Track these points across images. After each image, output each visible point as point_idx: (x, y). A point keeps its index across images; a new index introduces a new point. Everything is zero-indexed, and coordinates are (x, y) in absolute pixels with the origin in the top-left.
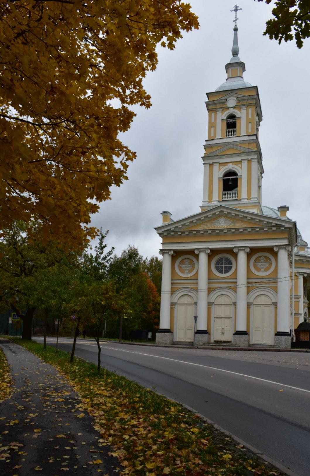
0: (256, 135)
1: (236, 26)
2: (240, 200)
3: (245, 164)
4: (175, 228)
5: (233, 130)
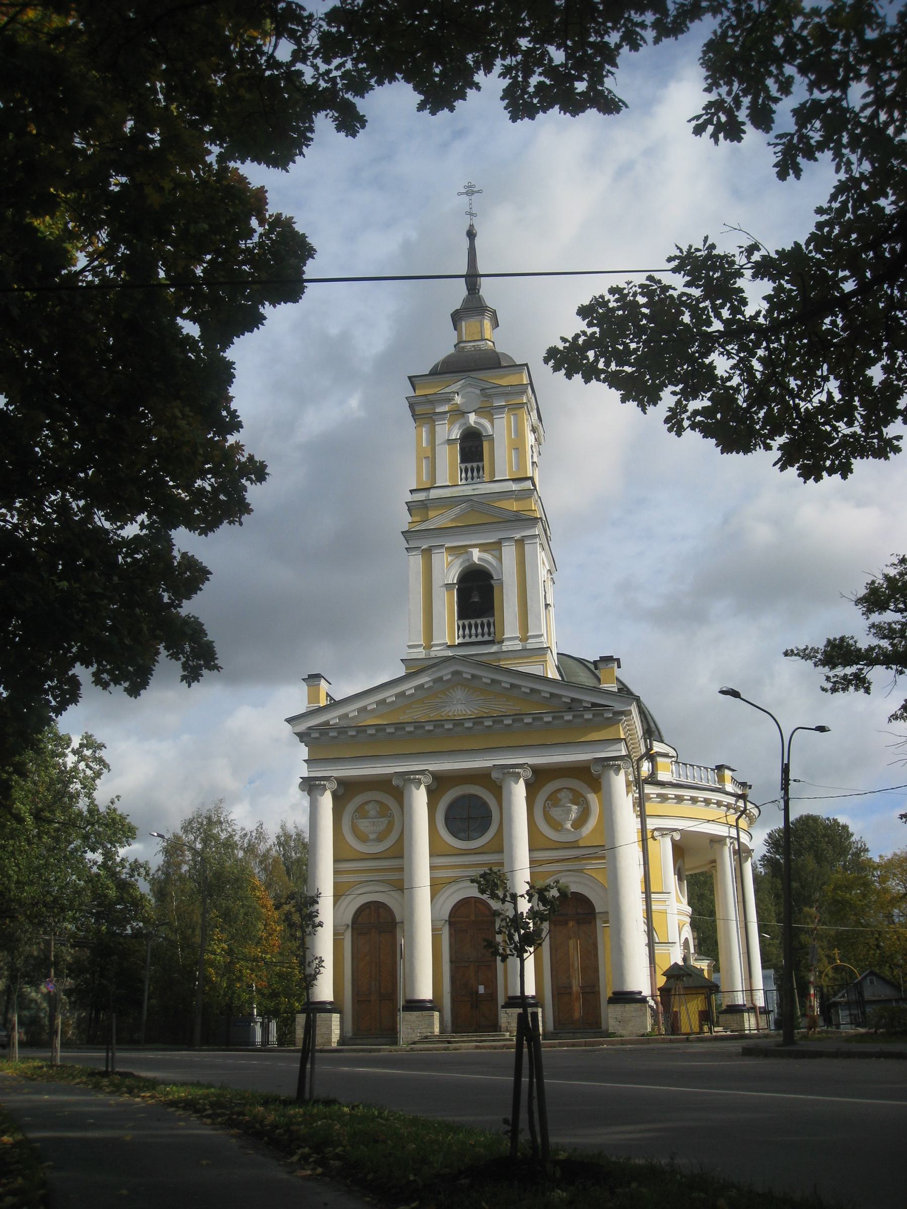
0: (531, 479)
1: (472, 226)
2: (501, 642)
3: (509, 552)
4: (340, 718)
5: (475, 465)
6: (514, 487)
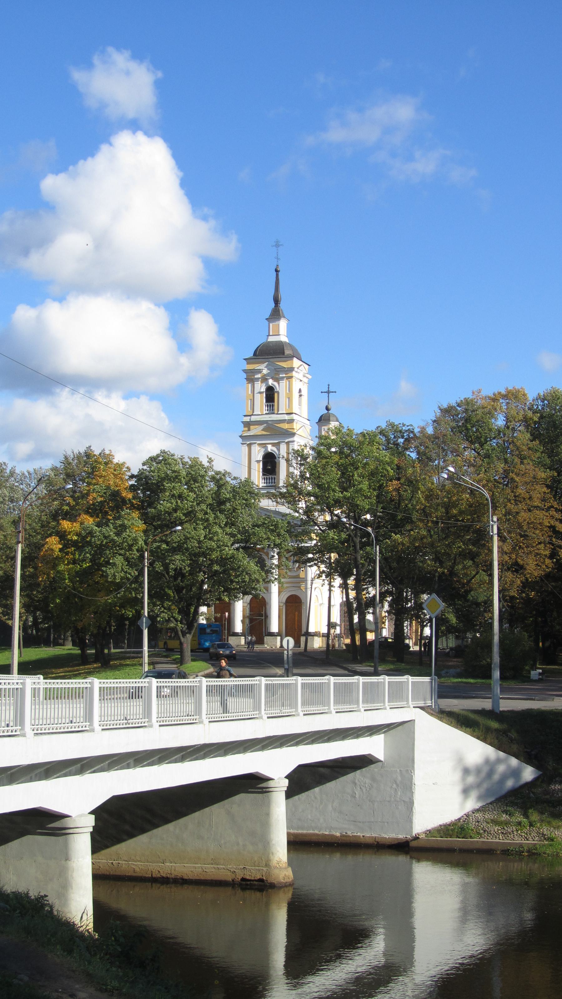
5: (271, 404)
6: (287, 417)
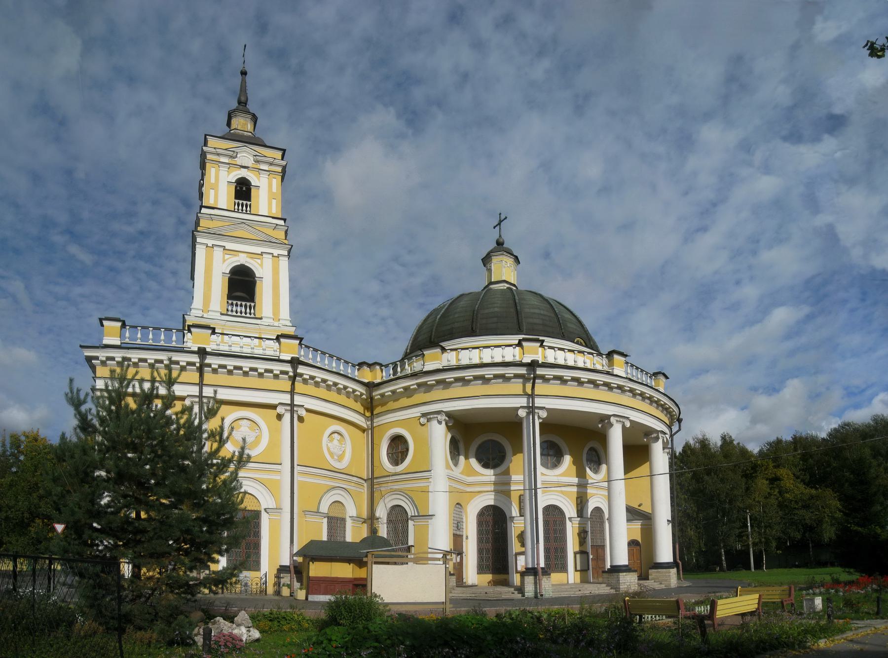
5: (245, 202)
